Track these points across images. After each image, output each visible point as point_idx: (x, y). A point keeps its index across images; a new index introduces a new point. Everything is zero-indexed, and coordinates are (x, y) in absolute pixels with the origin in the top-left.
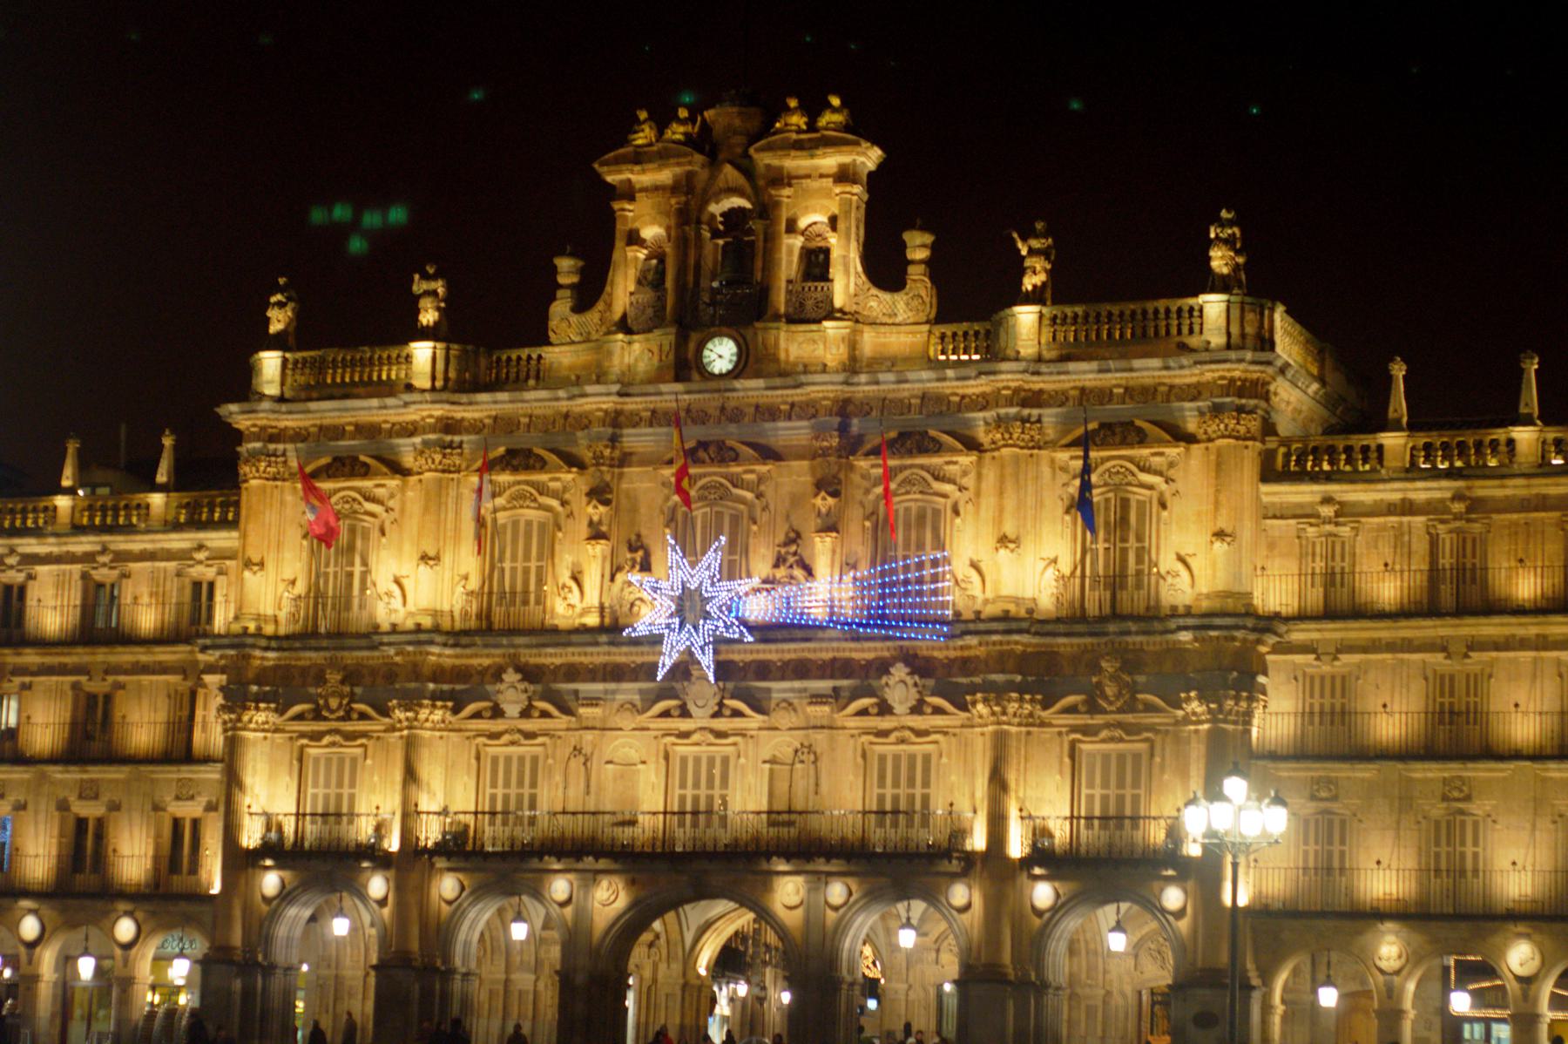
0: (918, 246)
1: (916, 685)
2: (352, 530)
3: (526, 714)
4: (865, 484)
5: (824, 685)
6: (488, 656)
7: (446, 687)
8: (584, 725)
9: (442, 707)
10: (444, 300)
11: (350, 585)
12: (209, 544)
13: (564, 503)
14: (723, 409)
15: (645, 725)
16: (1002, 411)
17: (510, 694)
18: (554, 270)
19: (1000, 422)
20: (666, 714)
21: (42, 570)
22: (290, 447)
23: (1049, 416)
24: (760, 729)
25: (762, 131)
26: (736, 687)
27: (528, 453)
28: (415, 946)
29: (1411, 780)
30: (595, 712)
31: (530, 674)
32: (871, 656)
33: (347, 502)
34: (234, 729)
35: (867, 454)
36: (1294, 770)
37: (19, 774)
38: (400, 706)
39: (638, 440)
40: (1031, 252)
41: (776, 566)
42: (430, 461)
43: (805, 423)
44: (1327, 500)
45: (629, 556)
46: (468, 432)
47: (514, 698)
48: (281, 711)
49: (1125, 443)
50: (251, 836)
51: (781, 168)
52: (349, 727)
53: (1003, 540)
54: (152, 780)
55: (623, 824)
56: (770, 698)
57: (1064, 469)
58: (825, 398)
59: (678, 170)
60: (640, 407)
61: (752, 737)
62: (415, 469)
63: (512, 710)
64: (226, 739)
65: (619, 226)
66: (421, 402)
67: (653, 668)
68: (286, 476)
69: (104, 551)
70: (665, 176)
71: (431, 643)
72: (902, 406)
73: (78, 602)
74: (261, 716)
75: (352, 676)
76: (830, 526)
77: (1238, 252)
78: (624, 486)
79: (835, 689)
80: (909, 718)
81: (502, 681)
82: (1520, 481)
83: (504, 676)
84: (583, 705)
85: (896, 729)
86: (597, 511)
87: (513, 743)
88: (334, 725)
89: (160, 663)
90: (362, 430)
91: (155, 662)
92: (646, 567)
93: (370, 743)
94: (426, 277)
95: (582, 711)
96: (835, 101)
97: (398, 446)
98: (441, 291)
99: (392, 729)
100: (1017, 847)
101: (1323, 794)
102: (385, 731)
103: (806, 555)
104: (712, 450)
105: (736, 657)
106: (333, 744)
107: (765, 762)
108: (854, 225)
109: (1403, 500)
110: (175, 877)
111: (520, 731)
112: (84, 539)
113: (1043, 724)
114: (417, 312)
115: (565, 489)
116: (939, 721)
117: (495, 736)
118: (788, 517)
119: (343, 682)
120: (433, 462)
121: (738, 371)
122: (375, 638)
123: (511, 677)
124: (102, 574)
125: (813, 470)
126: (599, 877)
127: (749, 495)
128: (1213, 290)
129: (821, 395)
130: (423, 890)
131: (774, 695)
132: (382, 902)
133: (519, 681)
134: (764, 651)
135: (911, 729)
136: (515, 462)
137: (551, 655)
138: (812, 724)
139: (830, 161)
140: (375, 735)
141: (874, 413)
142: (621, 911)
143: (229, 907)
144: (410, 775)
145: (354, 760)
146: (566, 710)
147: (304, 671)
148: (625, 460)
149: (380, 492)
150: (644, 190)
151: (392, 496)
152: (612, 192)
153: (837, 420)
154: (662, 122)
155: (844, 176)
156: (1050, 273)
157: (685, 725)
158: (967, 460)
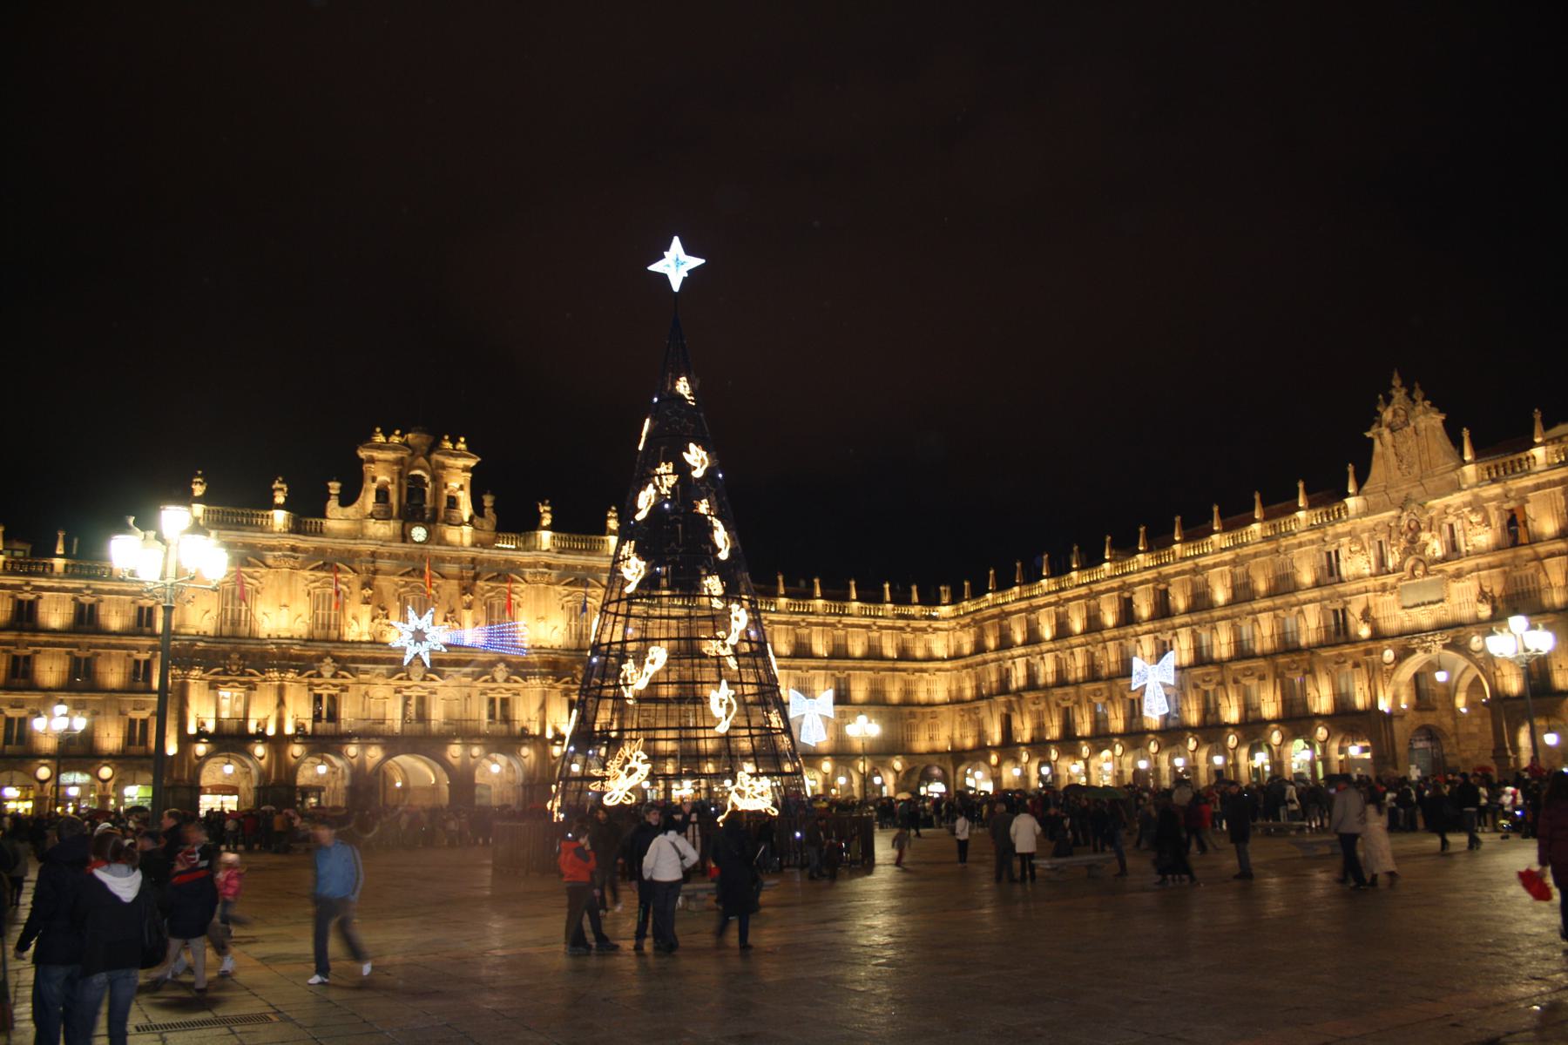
0: (488, 501)
3: (335, 676)
7: (294, 663)
11: (240, 615)
13: (349, 588)
16: (541, 570)
18: (328, 488)
19: (535, 574)
20: (401, 679)
21: (46, 594)
25: (435, 446)
27: (331, 565)
28: (283, 775)
30: (368, 676)
31: (336, 659)
32: (486, 659)
34: (185, 678)
37: (37, 696)
39: (384, 564)
40: (545, 511)
41: (446, 620)
45: (380, 612)
46: (301, 552)
48: (204, 672)
49: (582, 586)
50: (192, 729)
51: (443, 463)
53: (542, 618)
54: (119, 701)
55: (380, 723)
57: (560, 594)
59: (399, 455)
63: (327, 674)
65: (368, 476)
67: (403, 660)
69: (88, 588)
70: (390, 456)
72: (497, 563)
73: (72, 612)
74: (196, 673)
75: (243, 656)
76: (469, 607)
77: (619, 522)
78: (376, 583)
79: (473, 673)
86: (368, 592)
87: (327, 689)
88: (234, 678)
92: (387, 618)
94: (280, 482)
95: (362, 676)
96: (462, 439)
98: (286, 489)
99: (265, 681)
100: (549, 735)
103: (457, 617)
104: (417, 572)
106: (233, 687)
108: (467, 489)
110: (132, 747)
112: (77, 581)
113: (554, 688)
114: (274, 497)
115: (349, 582)
116: (516, 685)
118: (449, 602)
119: (239, 659)
121: (428, 540)
123: (328, 660)
124: (87, 599)
125: (460, 585)
127: (433, 592)
128: (610, 534)
131: (447, 673)
132: (261, 758)
136: (326, 568)
139: (461, 462)
143: (183, 760)
144: (281, 703)
146: (353, 676)
147: (216, 653)
148: (375, 572)
150: (379, 461)
151: (262, 577)
152: (361, 461)
153: (471, 566)
154: (387, 436)
155: (466, 469)
156: (552, 520)
158: (523, 586)
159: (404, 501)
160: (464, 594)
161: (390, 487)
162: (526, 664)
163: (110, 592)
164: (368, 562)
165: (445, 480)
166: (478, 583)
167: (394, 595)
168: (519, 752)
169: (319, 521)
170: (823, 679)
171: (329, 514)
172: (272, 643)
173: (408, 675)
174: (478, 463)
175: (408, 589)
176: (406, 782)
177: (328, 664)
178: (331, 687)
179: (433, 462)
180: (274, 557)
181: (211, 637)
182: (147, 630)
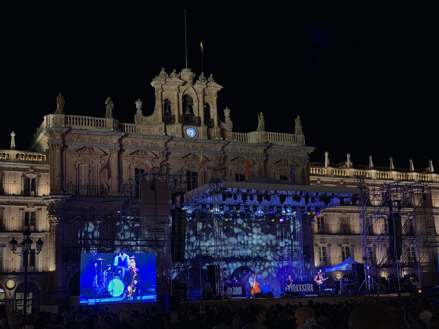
0: (227, 112)
12: (34, 167)
18: (136, 105)
29: (337, 239)
36: (319, 236)
44: (319, 180)
64: (50, 225)
82: (353, 179)
89: (18, 202)
91: (16, 202)
96: (211, 75)
101: (323, 242)
104: (192, 156)
109: (332, 181)
136: (139, 153)
141: (230, 151)
154: (169, 72)
159: (181, 113)
163: (9, 169)
169: (131, 125)
170: (419, 220)
171: (136, 122)
174: (222, 89)
182: (33, 193)
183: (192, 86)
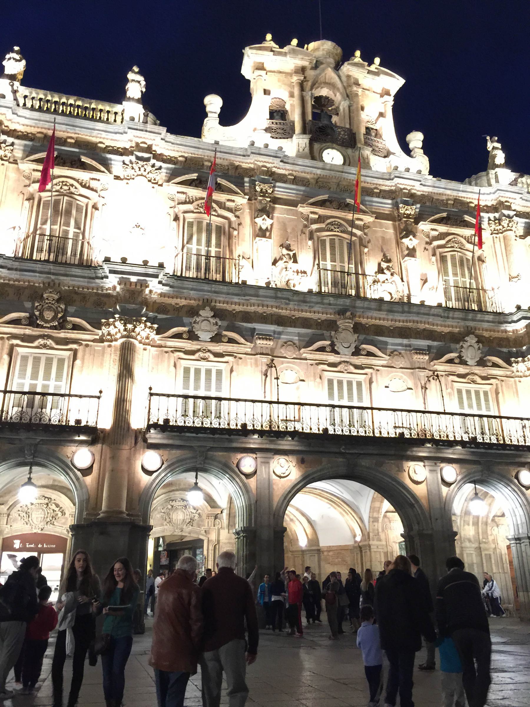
1: (479, 349)
2: (70, 204)
4: (428, 240)
5: (423, 343)
6: (186, 299)
8: (259, 351)
9: (150, 328)
10: (147, 86)
14: (338, 185)
15: (304, 355)
16: (506, 212)
17: (204, 325)
20: (322, 349)
22: (17, 141)
23: (521, 223)
24: (382, 366)
26: (365, 339)
28: (124, 508)
30: (271, 343)
31: (218, 314)
32: (447, 330)
33: (66, 185)
35: (433, 221)
38: (121, 319)
42: (142, 169)
43: (390, 201)
45: (285, 251)
46: (164, 161)
47: (208, 329)
52: (62, 334)
56: (386, 349)
58: (404, 189)
60: (287, 173)
61: (378, 370)
62: (122, 177)
63: (205, 336)
66: (142, 130)
68: (11, 160)
71: (156, 276)
72: (445, 203)
79: (429, 347)
80: (477, 368)
81: (198, 315)
83: (201, 312)
84: (260, 338)
85: (467, 374)
86: (263, 222)
87: (204, 359)
90: (79, 143)
93: (80, 349)
95: (258, 342)
97: (111, 160)
98: (143, 83)
102: (94, 341)
103: (396, 269)
105: (364, 321)
106: (45, 346)
107: (387, 387)
111: (209, 351)
117: (193, 353)
119: (58, 301)
120: (145, 171)
122: (106, 268)
123: (206, 313)
126: (277, 457)
129: (402, 187)
130: (130, 461)
132: (87, 471)
133: (212, 317)
134: (384, 320)
135: (476, 374)
137: (236, 304)
138: (417, 365)
140: (84, 343)
141: (428, 204)
142: (296, 482)
145: (61, 361)
149: (93, 184)
157: (332, 358)
159: (310, 117)
160: (406, 236)
161: (288, 107)
162: (505, 341)
164: (264, 181)
165: (361, 103)
166: (424, 226)
167: (303, 232)
168: (517, 477)
172: (112, 272)
173: (333, 345)
175: (323, 225)
176: (314, 541)
177: (206, 319)
178: (212, 358)
179: (344, 79)
180: (124, 163)
181: (9, 258)
183: (337, 72)
